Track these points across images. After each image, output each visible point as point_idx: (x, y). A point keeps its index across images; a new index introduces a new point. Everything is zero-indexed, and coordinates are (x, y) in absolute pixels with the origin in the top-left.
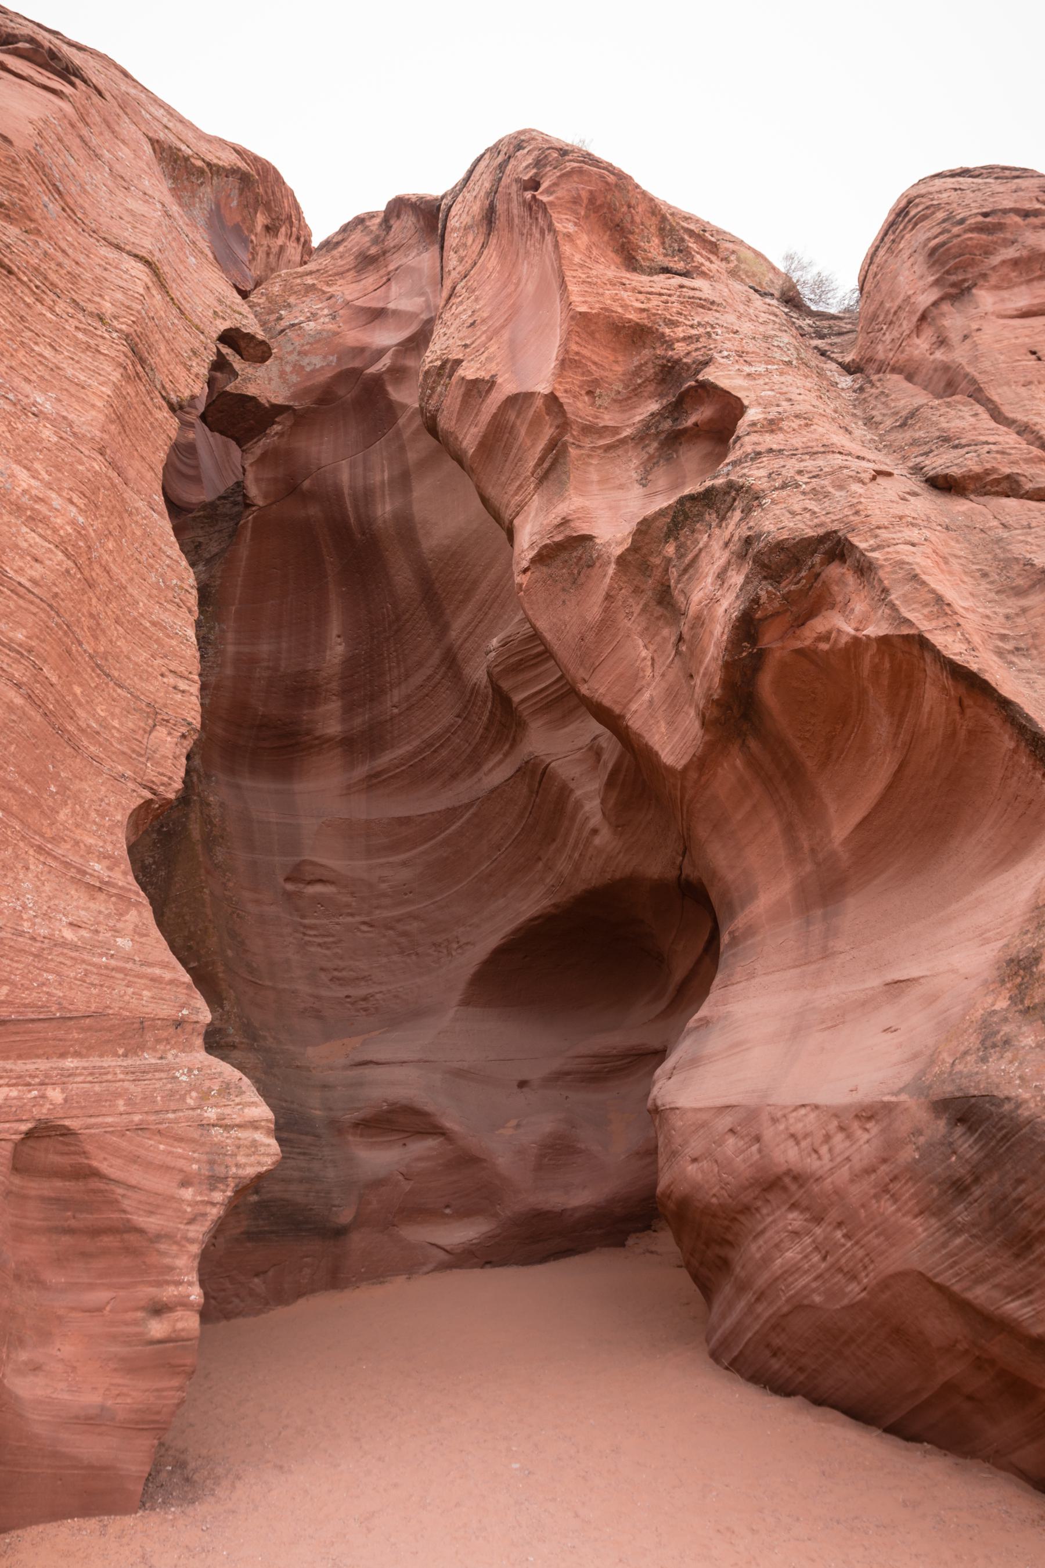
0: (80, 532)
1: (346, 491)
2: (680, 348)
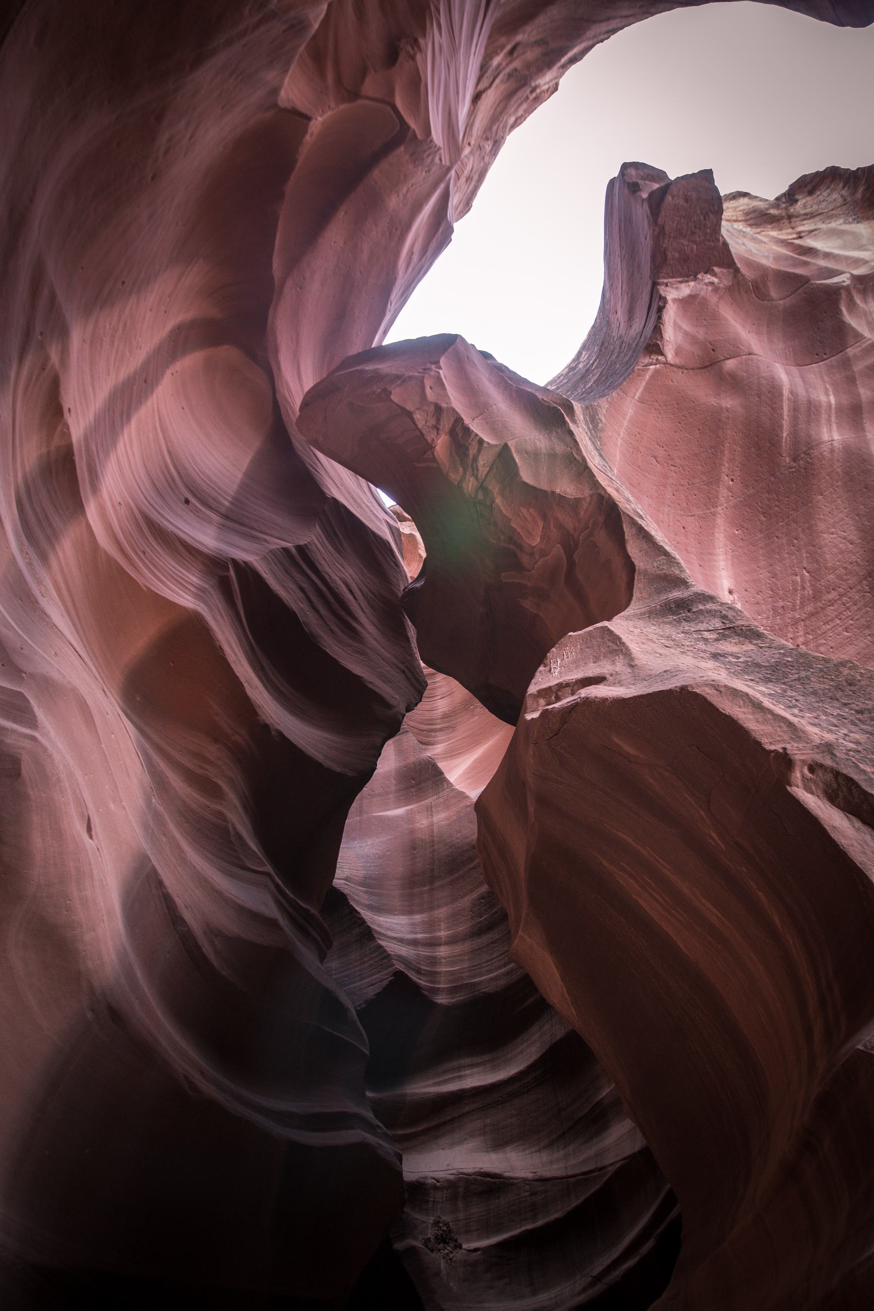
1: (786, 393)
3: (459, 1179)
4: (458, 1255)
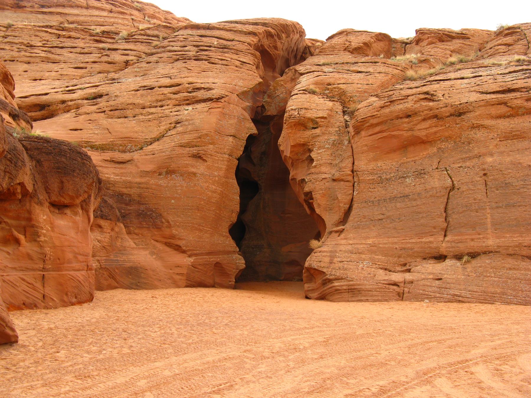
0: (221, 191)
2: (310, 147)
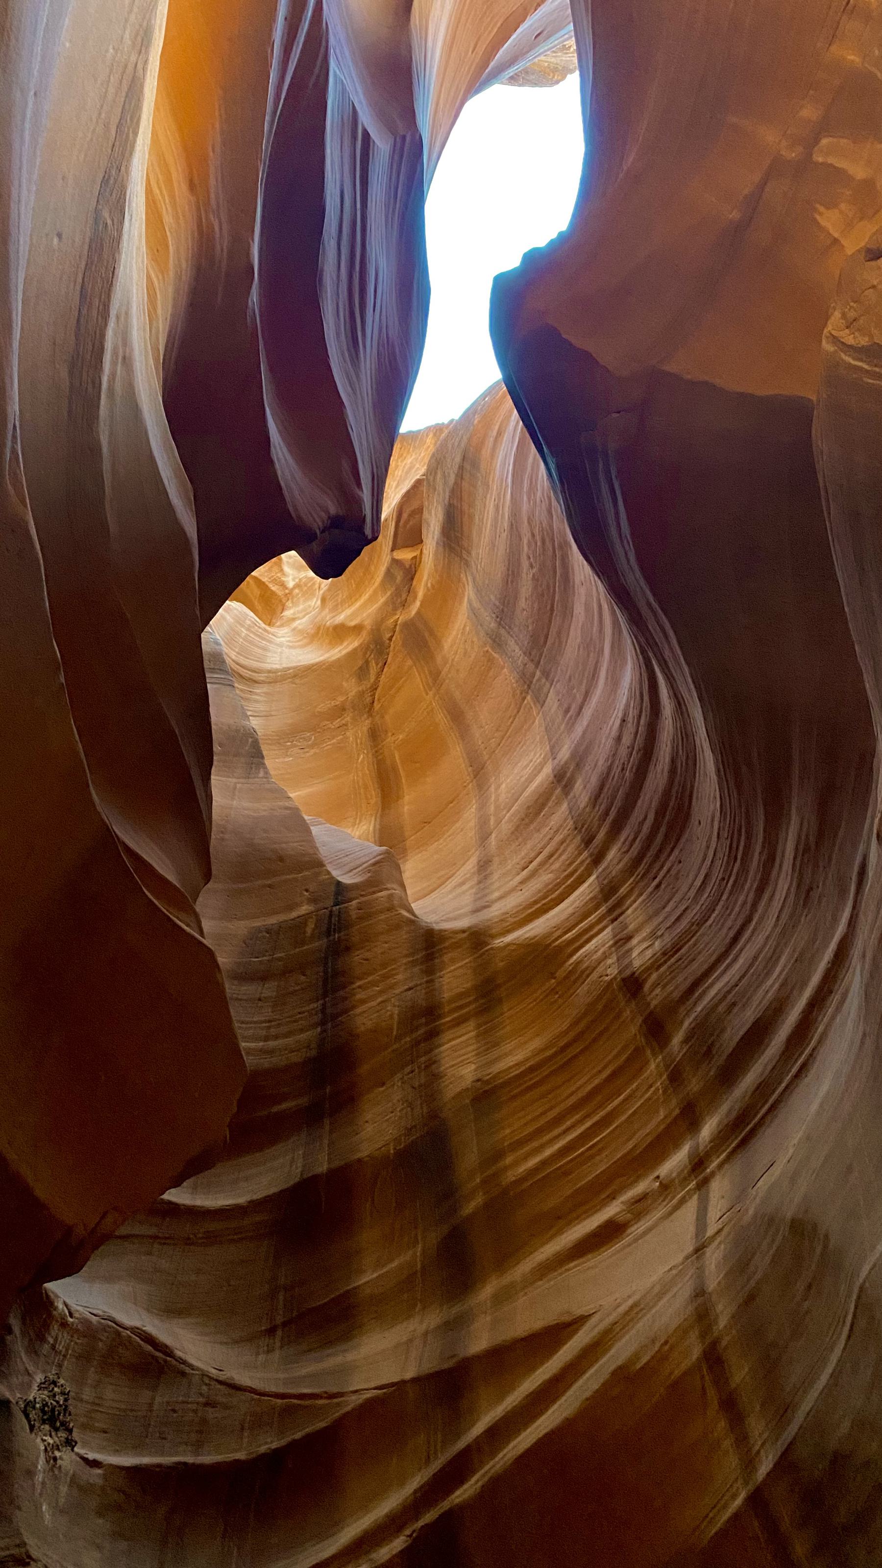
3: (105, 1328)
4: (66, 1458)
